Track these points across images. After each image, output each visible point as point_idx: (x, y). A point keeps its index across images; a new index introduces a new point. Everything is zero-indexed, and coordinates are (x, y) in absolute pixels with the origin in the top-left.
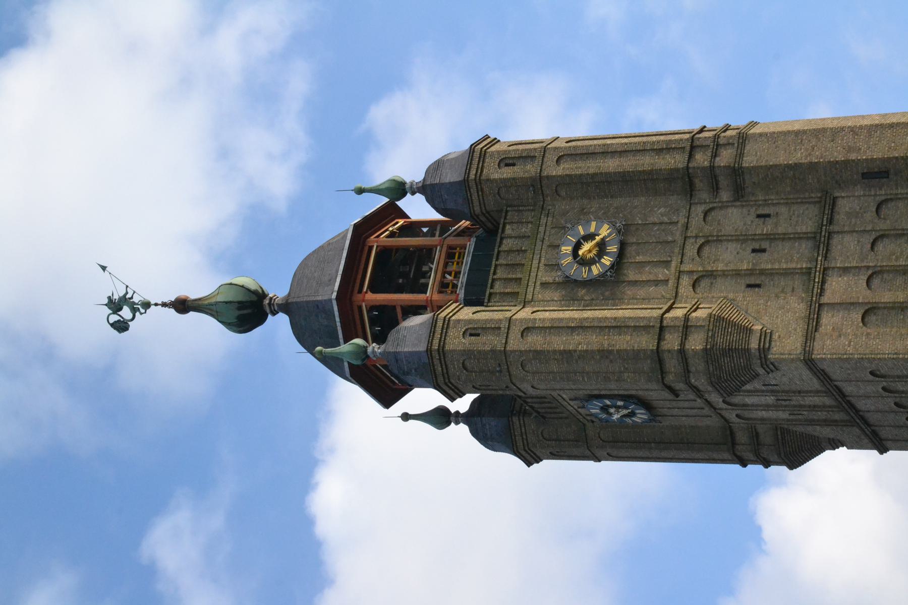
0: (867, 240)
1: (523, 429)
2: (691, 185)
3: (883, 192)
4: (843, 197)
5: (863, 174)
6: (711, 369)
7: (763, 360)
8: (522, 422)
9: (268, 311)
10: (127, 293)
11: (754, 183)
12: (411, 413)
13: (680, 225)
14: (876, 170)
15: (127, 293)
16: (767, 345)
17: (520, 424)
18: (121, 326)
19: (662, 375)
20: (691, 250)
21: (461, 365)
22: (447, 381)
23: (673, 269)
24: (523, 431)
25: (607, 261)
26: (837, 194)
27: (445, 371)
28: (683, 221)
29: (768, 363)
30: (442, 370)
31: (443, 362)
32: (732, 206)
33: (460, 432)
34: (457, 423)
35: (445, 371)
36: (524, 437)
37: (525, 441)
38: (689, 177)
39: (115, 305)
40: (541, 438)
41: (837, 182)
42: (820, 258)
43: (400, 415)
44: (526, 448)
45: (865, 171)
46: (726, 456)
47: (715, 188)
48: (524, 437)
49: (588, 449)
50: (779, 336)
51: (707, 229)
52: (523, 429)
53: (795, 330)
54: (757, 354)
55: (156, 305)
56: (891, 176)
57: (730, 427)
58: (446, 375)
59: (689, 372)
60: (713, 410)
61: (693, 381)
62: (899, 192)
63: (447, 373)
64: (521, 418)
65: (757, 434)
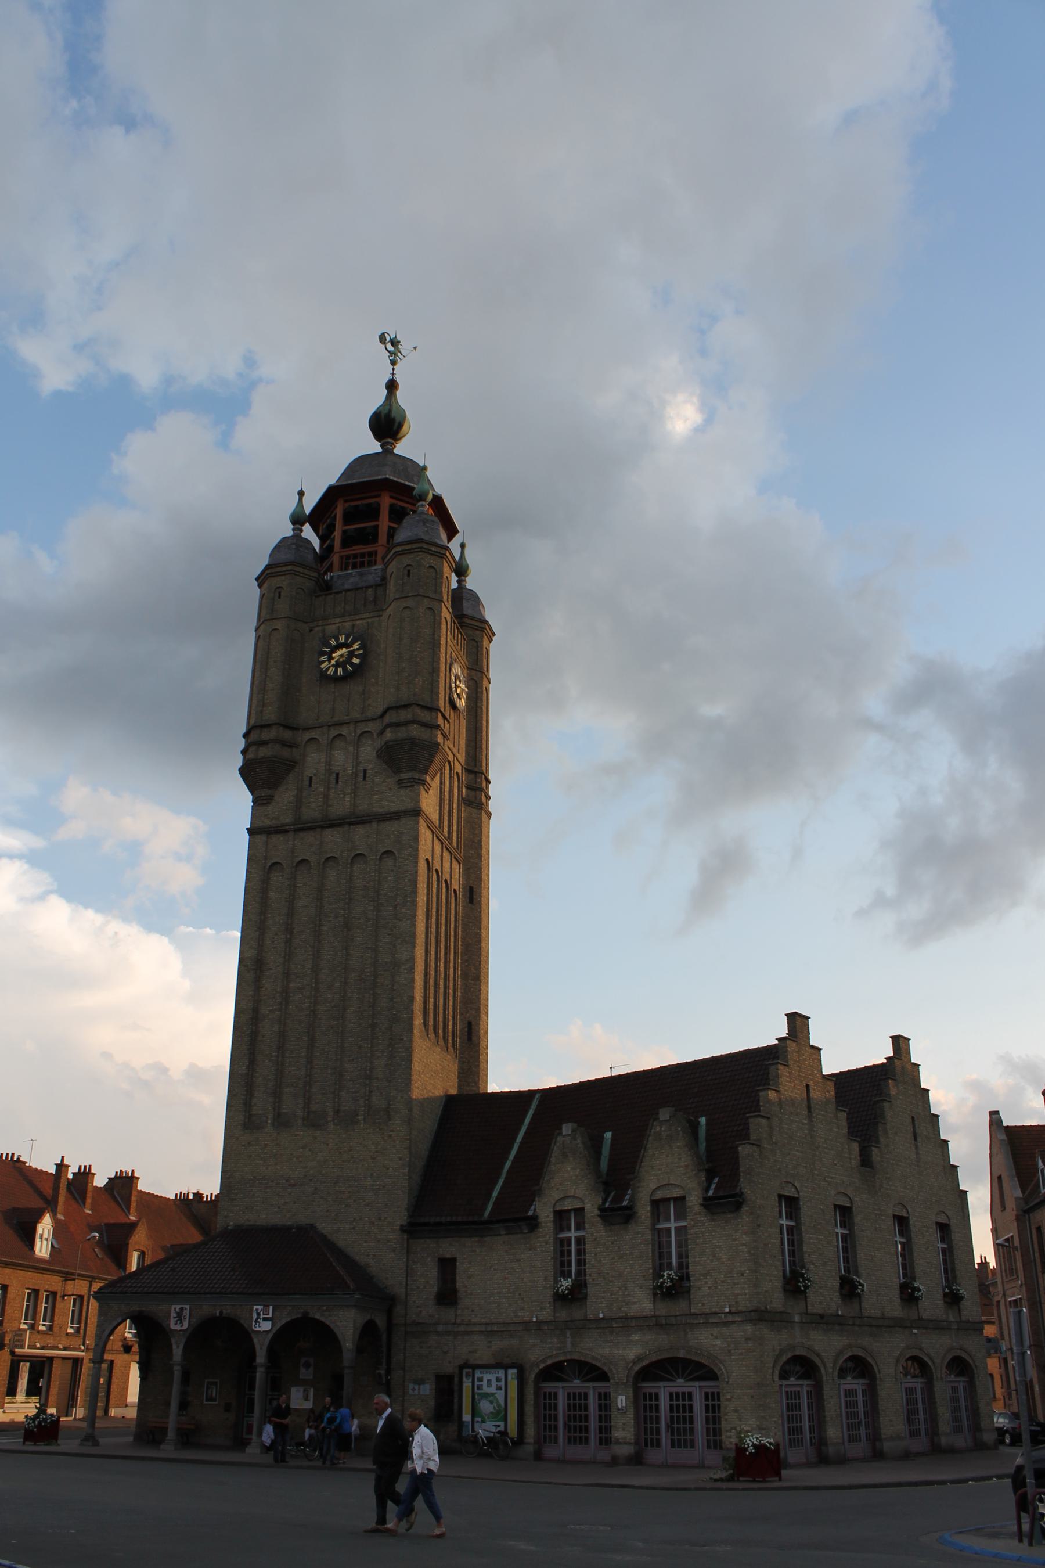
7: (417, 781)
9: (384, 441)
10: (401, 354)
12: (304, 497)
14: (474, 897)
15: (401, 354)
16: (426, 788)
17: (306, 575)
18: (382, 338)
21: (433, 565)
22: (423, 550)
27: (430, 552)
29: (413, 783)
30: (432, 551)
31: (437, 554)
34: (293, 530)
35: (430, 552)
39: (394, 343)
43: (303, 490)
44: (293, 572)
45: (474, 890)
46: (271, 714)
49: (287, 617)
54: (423, 779)
55: (393, 369)
57: (297, 729)
58: (427, 551)
60: (329, 724)
61: (415, 726)
63: (428, 553)
65: (290, 746)
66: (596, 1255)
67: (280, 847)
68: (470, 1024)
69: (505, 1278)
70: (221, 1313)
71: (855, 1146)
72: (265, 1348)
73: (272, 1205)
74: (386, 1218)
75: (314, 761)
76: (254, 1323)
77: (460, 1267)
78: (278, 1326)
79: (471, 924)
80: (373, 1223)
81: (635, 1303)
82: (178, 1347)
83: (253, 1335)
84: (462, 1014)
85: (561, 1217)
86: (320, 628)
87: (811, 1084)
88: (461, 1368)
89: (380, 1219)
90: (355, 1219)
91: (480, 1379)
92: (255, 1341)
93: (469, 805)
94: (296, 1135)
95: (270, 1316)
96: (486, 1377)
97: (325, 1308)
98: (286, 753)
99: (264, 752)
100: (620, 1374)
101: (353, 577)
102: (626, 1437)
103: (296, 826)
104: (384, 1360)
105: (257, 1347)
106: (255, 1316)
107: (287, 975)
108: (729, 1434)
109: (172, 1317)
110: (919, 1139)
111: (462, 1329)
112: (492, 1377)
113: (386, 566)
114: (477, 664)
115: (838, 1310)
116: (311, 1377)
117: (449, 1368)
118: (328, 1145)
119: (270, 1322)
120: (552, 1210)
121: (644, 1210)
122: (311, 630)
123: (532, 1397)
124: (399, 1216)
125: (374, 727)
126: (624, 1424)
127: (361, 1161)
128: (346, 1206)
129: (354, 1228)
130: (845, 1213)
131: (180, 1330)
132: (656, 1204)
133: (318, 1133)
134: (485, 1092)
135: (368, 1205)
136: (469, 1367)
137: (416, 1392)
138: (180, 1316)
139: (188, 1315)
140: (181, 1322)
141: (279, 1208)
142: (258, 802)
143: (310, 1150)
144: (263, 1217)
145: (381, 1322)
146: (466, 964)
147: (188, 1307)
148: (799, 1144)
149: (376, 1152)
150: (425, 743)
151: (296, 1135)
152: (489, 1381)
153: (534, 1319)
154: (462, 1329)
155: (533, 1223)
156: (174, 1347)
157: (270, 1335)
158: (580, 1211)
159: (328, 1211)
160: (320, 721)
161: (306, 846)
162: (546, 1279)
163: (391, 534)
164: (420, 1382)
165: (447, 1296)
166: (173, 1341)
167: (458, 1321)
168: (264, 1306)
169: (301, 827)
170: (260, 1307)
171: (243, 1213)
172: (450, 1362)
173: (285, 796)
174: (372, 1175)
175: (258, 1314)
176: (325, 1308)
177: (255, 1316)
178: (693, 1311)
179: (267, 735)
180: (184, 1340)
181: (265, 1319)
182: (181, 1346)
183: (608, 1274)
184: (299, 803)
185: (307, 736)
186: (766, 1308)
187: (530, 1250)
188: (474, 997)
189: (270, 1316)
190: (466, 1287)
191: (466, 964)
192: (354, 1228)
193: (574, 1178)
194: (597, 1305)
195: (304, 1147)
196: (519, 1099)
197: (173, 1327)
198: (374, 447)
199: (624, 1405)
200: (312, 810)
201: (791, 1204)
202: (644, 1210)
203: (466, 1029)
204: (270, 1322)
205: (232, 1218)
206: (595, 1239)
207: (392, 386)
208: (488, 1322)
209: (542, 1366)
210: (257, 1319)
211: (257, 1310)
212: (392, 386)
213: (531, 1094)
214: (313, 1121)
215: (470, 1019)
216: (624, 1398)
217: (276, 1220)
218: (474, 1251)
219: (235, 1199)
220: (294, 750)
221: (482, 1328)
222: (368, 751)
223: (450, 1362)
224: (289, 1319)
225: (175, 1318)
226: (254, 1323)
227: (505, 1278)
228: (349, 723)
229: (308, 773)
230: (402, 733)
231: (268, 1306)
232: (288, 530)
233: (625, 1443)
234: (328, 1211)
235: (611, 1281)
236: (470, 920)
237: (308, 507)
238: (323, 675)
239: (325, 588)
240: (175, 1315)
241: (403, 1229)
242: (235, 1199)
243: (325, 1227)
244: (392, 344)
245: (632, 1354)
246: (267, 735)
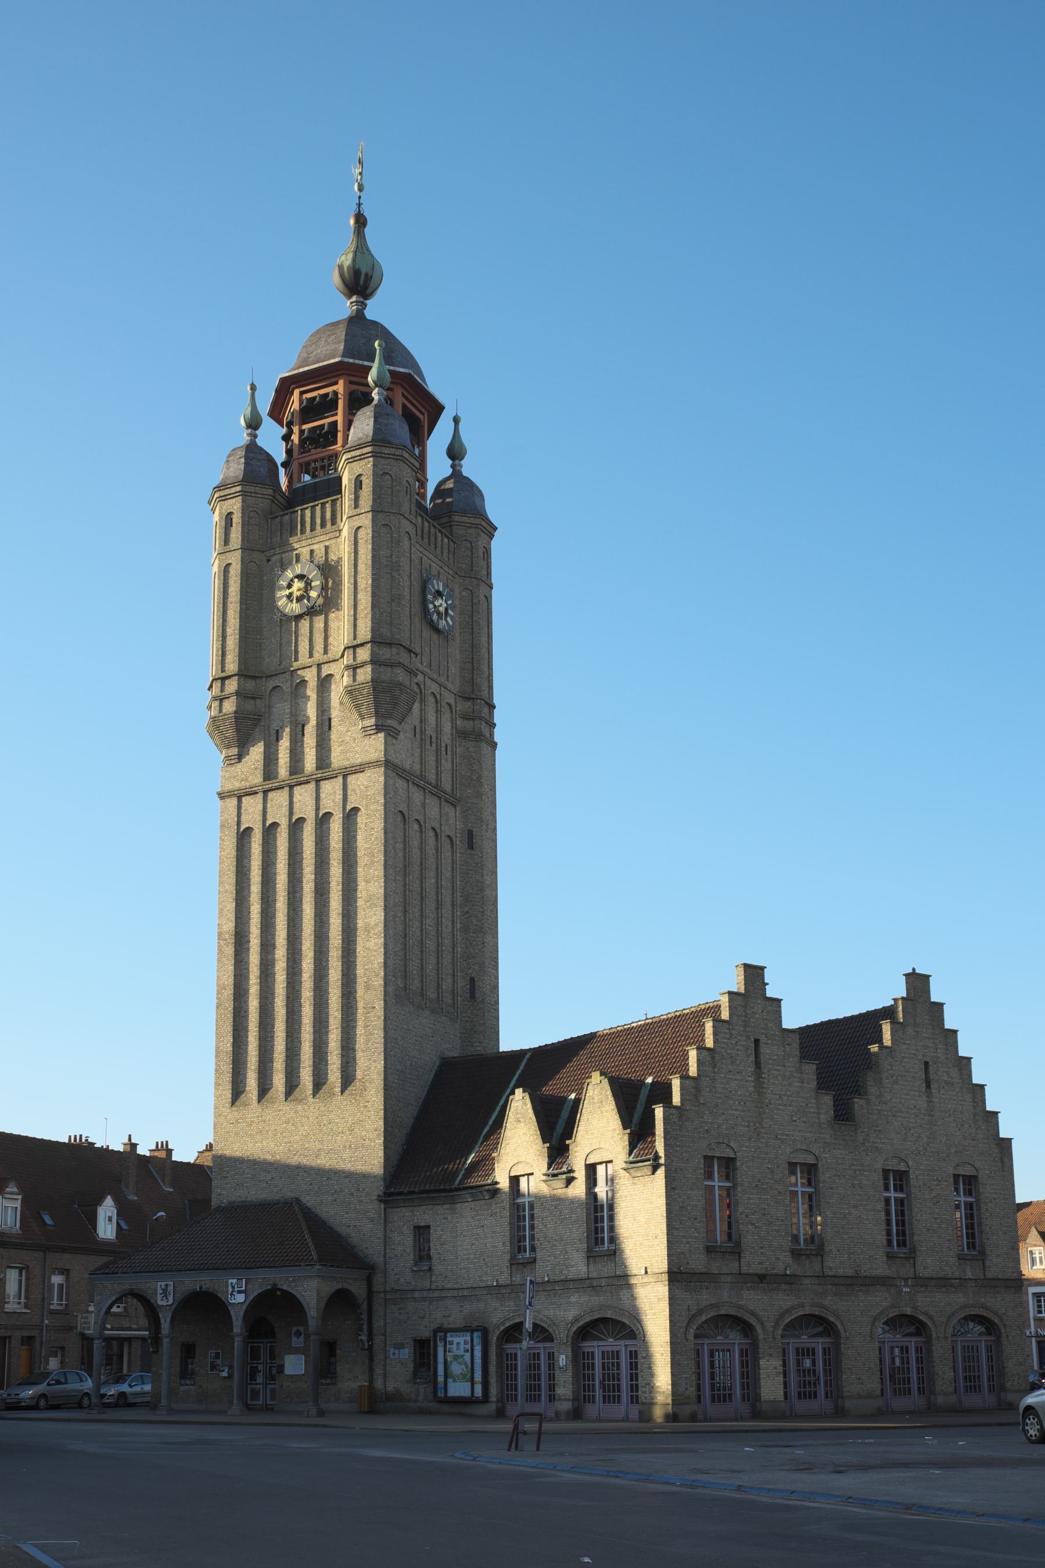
0: (436, 826)
1: (261, 496)
2: (468, 699)
3: (458, 843)
4: (455, 813)
5: (472, 831)
6: (384, 685)
8: (266, 497)
11: (469, 748)
13: (447, 682)
14: (474, 841)
19: (377, 642)
20: (434, 687)
23: (426, 670)
24: (259, 496)
25: (435, 617)
26: (457, 807)
28: (450, 686)
32: (452, 727)
33: (245, 438)
36: (253, 495)
37: (249, 494)
38: (474, 699)
40: (251, 509)
41: (467, 810)
42: (431, 787)
45: (474, 833)
47: (465, 717)
48: (253, 495)
50: (394, 744)
51: (444, 704)
52: (261, 496)
53: (397, 758)
56: (469, 851)
57: (261, 677)
59: (380, 665)
62: (458, 855)
64: (271, 497)
66: (543, 1220)
68: (472, 980)
69: (473, 1244)
70: (201, 1288)
71: (828, 1100)
72: (241, 1318)
73: (260, 1181)
74: (364, 1189)
76: (230, 1296)
77: (435, 1234)
78: (251, 1298)
79: (470, 872)
80: (353, 1194)
81: (573, 1266)
82: (165, 1321)
83: (230, 1308)
84: (463, 971)
86: (278, 557)
87: (762, 1038)
88: (435, 1332)
89: (358, 1190)
90: (335, 1191)
91: (451, 1343)
92: (232, 1313)
93: (465, 738)
94: (280, 1110)
95: (244, 1288)
96: (456, 1340)
97: (291, 1279)
102: (566, 1394)
103: (264, 787)
104: (365, 1327)
105: (234, 1318)
106: (230, 1290)
108: (644, 1389)
109: (158, 1294)
110: (934, 1086)
111: (436, 1294)
112: (461, 1340)
114: (472, 570)
115: (786, 1269)
116: (302, 1345)
117: (425, 1333)
118: (308, 1118)
119: (244, 1295)
120: (508, 1175)
122: (268, 561)
123: (495, 1358)
126: (564, 1382)
127: (340, 1133)
128: (328, 1179)
129: (336, 1200)
131: (167, 1305)
133: (300, 1107)
134: (495, 1051)
135: (347, 1177)
136: (442, 1331)
137: (397, 1356)
139: (172, 1292)
140: (167, 1298)
141: (267, 1183)
143: (293, 1125)
145: (358, 1289)
146: (466, 916)
147: (171, 1283)
148: (739, 1103)
149: (354, 1124)
150: (384, 685)
151: (280, 1110)
152: (458, 1343)
153: (495, 1284)
154: (436, 1294)
156: (162, 1321)
157: (245, 1307)
159: (311, 1184)
160: (282, 666)
162: (504, 1243)
164: (400, 1346)
166: (161, 1315)
167: (433, 1287)
168: (238, 1279)
170: (234, 1281)
171: (235, 1190)
172: (426, 1327)
174: (350, 1146)
175: (233, 1287)
176: (291, 1279)
177: (230, 1290)
178: (617, 1273)
180: (170, 1315)
181: (239, 1292)
182: (169, 1319)
183: (552, 1237)
185: (271, 684)
186: (679, 1269)
187: (491, 1216)
188: (476, 951)
189: (244, 1288)
190: (439, 1253)
191: (466, 916)
192: (336, 1200)
193: (525, 1143)
194: (543, 1271)
195: (287, 1123)
196: (517, 1056)
197: (160, 1303)
199: (565, 1364)
203: (468, 987)
204: (244, 1295)
206: (542, 1204)
208: (460, 1286)
209: (502, 1328)
210: (232, 1292)
211: (232, 1283)
215: (473, 975)
216: (564, 1357)
218: (447, 1218)
219: (227, 1177)
220: (258, 701)
221: (454, 1293)
223: (426, 1327)
224: (260, 1291)
225: (161, 1294)
226: (230, 1296)
227: (473, 1244)
228: (311, 666)
231: (242, 1279)
233: (566, 1400)
234: (311, 1184)
235: (555, 1245)
236: (470, 868)
240: (161, 1292)
241: (380, 1200)
242: (227, 1177)
245: (570, 1315)
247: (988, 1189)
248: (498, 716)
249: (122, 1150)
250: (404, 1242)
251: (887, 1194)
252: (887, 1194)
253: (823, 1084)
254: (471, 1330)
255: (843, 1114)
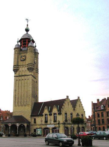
18: (26, 19)
46: (16, 64)
67: (17, 78)
75: (20, 69)
85: (45, 115)
98: (18, 68)
99: (15, 68)
100: (51, 129)
101: (24, 49)
107: (19, 91)
113: (27, 48)
121: (53, 114)
124: (30, 114)
125: (27, 66)
130: (71, 114)
132: (54, 114)
138: (10, 125)
142: (15, 73)
144: (17, 115)
145: (29, 124)
155: (43, 115)
158: (47, 114)
161: (20, 78)
163: (28, 44)
165: (35, 122)
169: (19, 76)
173: (18, 73)
179: (15, 67)
184: (19, 74)
194: (49, 122)
196: (42, 103)
198: (26, 33)
200: (20, 74)
201: (66, 114)
202: (53, 114)
205: (14, 115)
207: (27, 25)
212: (27, 25)
213: (42, 103)
214: (22, 106)
217: (18, 115)
222: (26, 68)
229: (20, 70)
230: (30, 67)
232: (17, 43)
237: (19, 40)
238: (21, 60)
239: (21, 50)
243: (23, 116)
244: (27, 20)
246: (15, 67)
247: (84, 115)
248: (39, 71)
249: (11, 111)
250: (33, 120)
251: (103, 118)
252: (99, 119)
253: (73, 107)
254: (40, 128)
255: (74, 110)
